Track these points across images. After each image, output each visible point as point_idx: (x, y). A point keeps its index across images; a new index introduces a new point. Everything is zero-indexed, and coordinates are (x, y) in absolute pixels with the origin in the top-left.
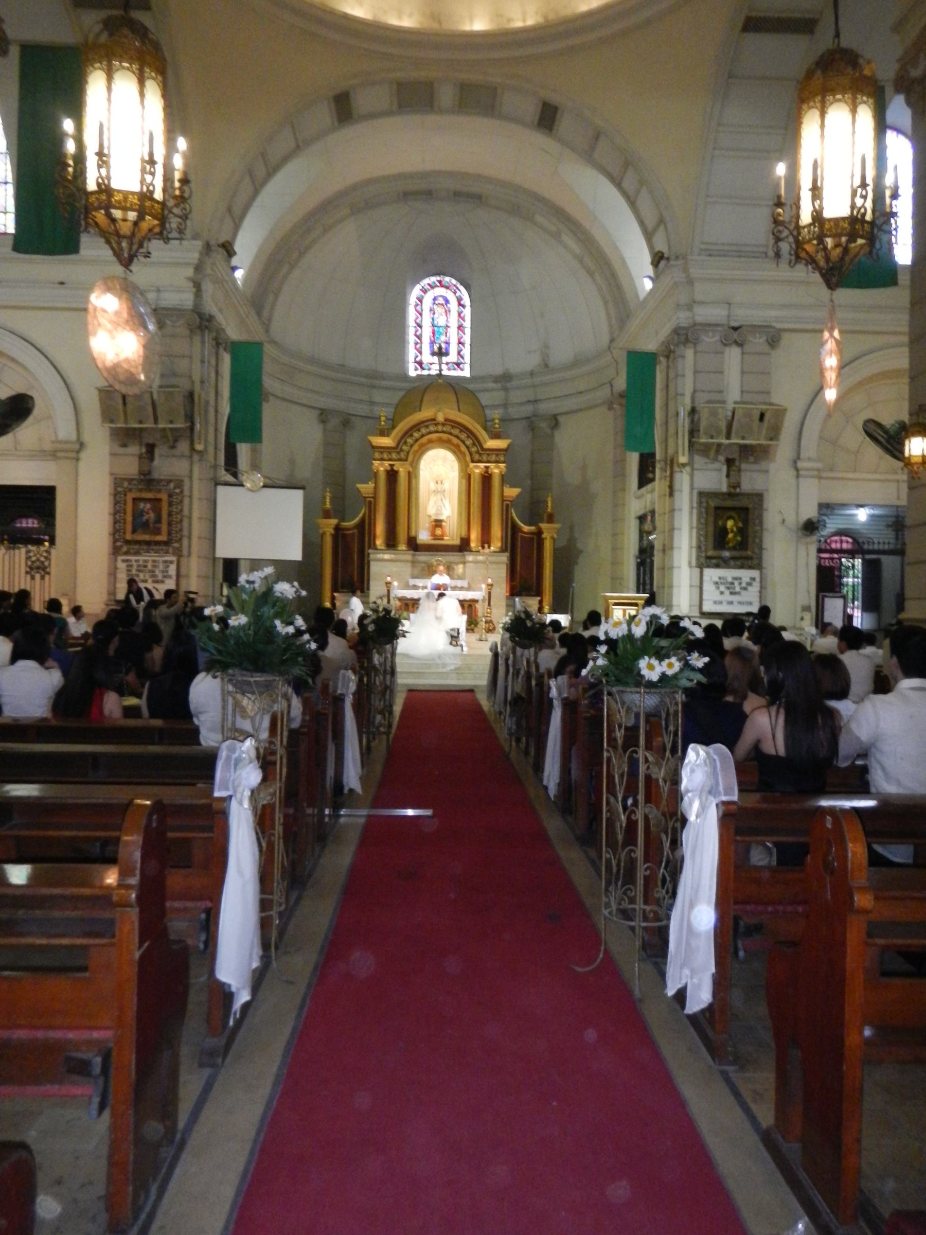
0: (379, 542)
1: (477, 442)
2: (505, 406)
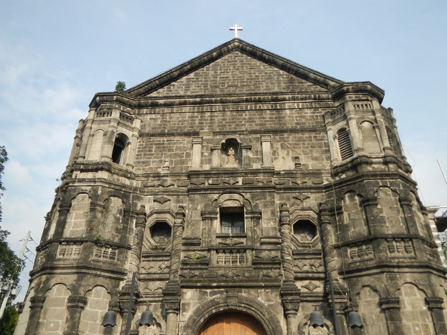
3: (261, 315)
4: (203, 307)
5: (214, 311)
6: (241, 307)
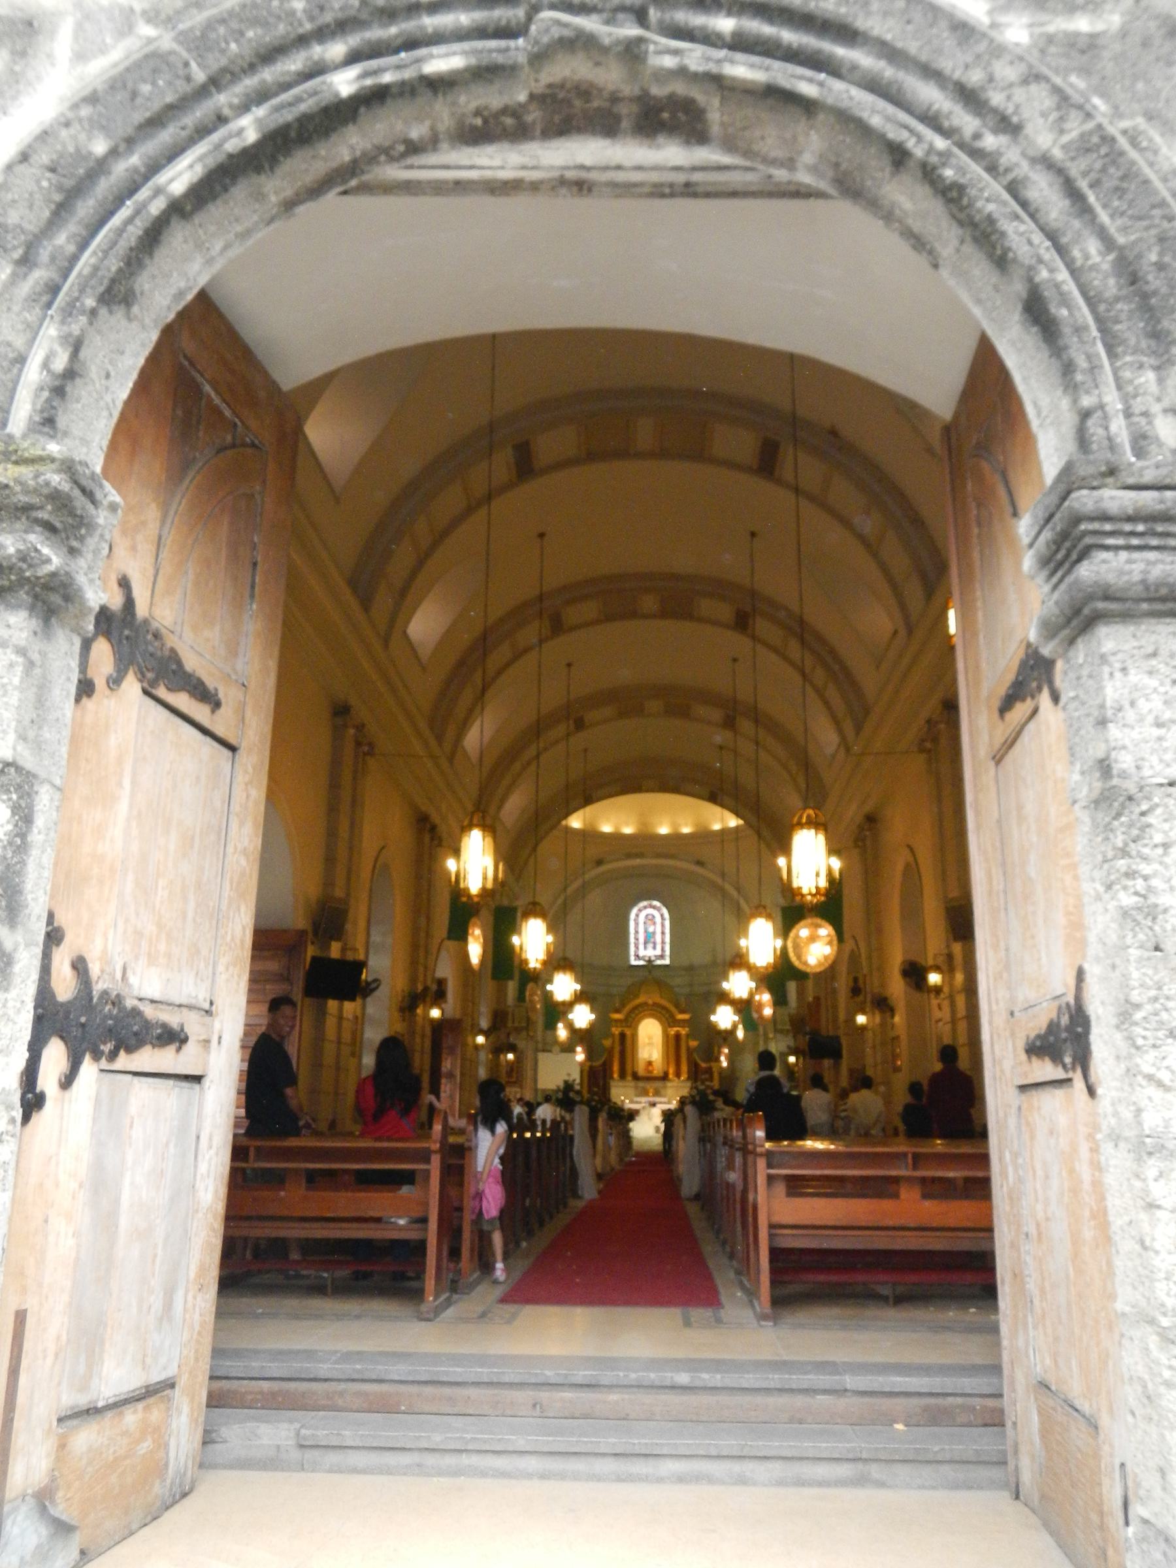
0: (616, 1076)
1: (672, 1016)
2: (691, 985)
3: (967, 122)
4: (200, 42)
5: (345, 83)
6: (709, 39)
